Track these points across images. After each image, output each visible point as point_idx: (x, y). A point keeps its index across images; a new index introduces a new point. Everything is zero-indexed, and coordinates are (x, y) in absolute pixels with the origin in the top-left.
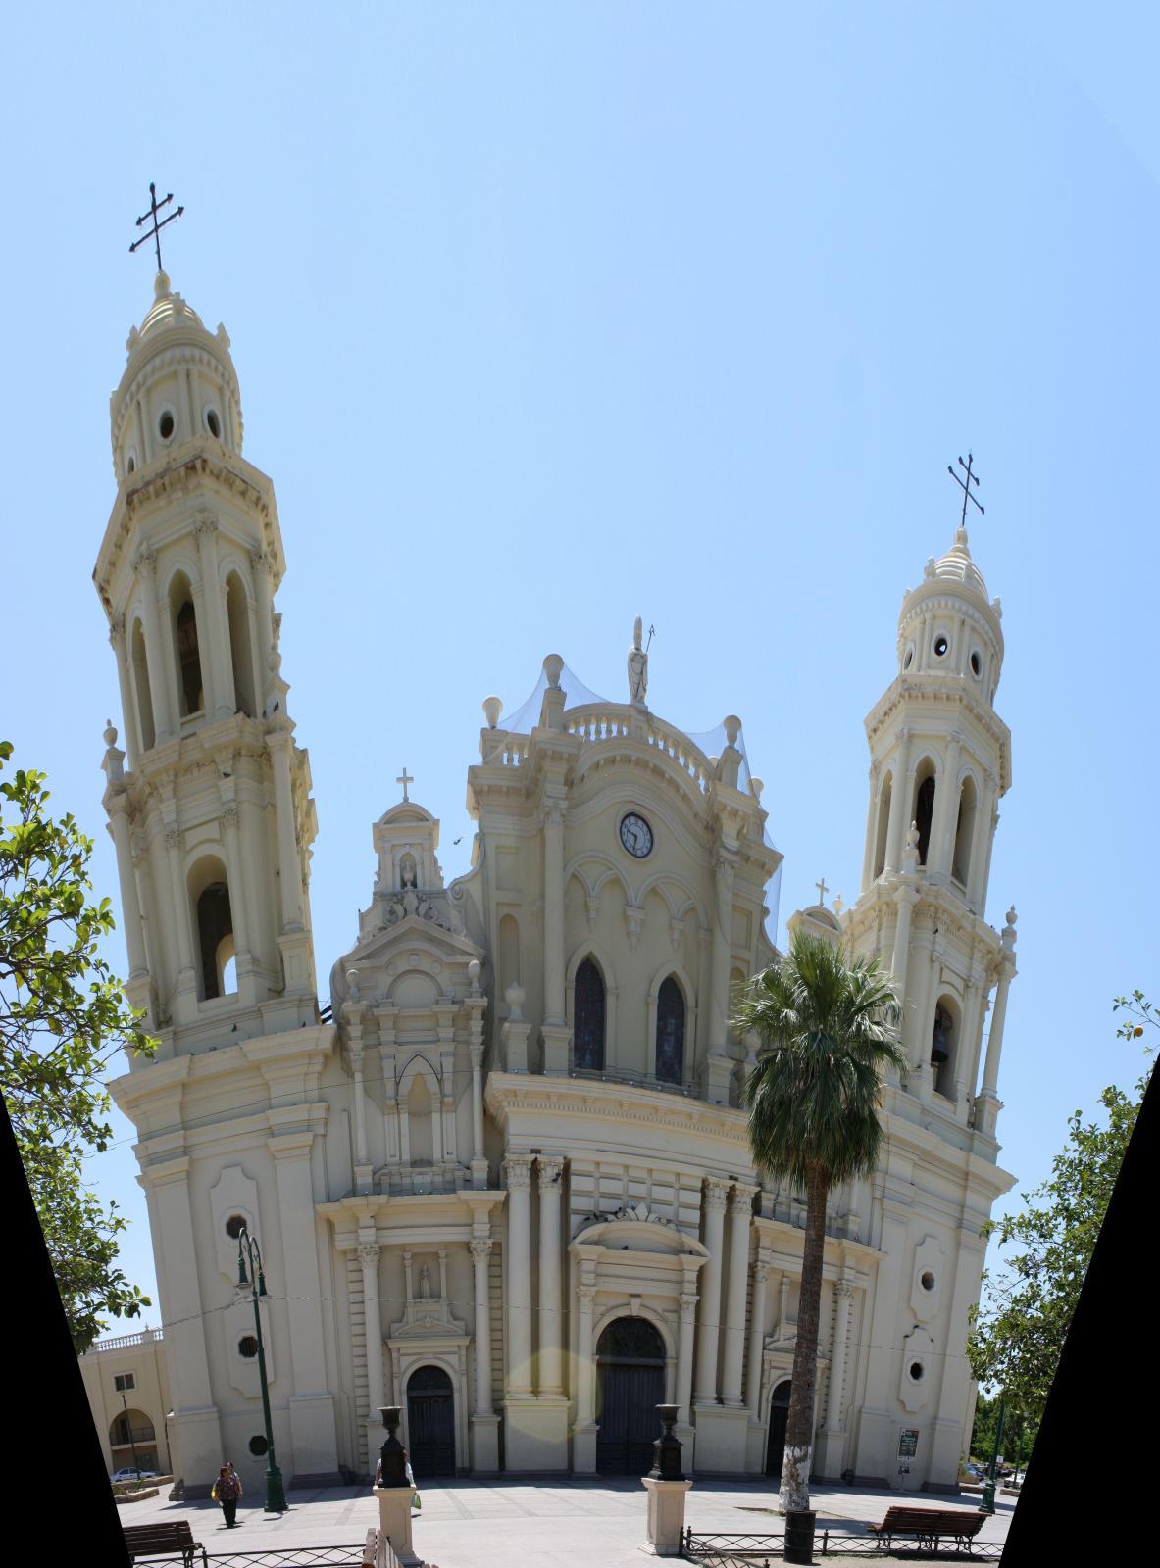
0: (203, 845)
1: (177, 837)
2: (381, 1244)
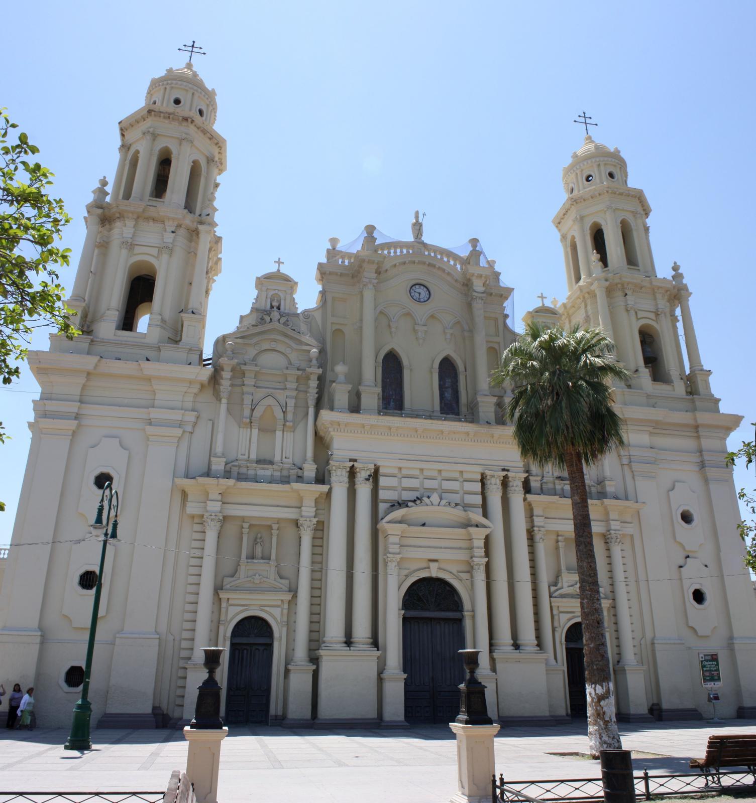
0: (146, 255)
1: (131, 246)
2: (225, 515)
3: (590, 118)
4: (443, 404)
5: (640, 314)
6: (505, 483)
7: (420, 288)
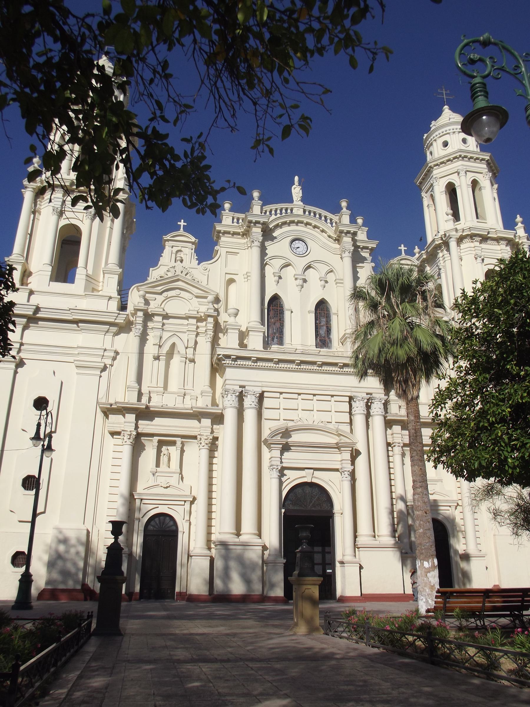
4: (318, 340)
5: (486, 261)
7: (299, 243)
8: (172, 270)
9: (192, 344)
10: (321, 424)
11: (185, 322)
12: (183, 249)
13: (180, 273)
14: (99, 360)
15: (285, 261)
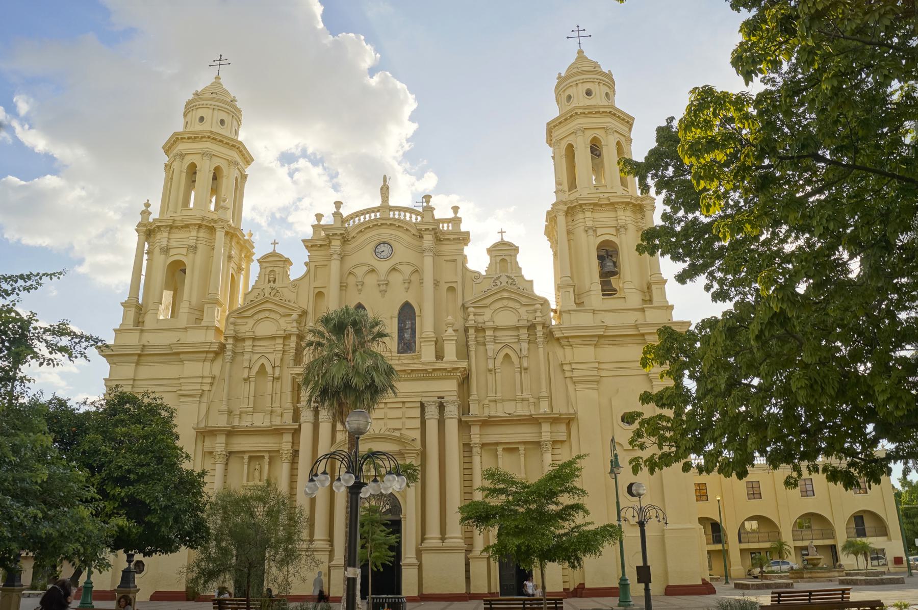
0: (177, 254)
1: (166, 250)
3: (584, 30)
5: (600, 231)
6: (441, 407)
8: (262, 294)
9: (278, 363)
10: (388, 433)
11: (272, 342)
12: (275, 269)
13: (269, 296)
14: (198, 387)
15: (368, 268)
